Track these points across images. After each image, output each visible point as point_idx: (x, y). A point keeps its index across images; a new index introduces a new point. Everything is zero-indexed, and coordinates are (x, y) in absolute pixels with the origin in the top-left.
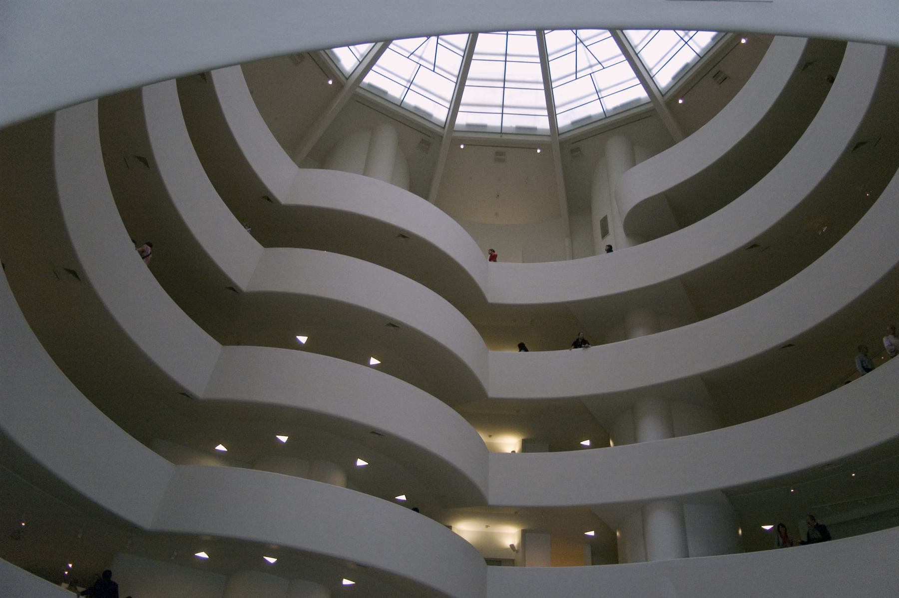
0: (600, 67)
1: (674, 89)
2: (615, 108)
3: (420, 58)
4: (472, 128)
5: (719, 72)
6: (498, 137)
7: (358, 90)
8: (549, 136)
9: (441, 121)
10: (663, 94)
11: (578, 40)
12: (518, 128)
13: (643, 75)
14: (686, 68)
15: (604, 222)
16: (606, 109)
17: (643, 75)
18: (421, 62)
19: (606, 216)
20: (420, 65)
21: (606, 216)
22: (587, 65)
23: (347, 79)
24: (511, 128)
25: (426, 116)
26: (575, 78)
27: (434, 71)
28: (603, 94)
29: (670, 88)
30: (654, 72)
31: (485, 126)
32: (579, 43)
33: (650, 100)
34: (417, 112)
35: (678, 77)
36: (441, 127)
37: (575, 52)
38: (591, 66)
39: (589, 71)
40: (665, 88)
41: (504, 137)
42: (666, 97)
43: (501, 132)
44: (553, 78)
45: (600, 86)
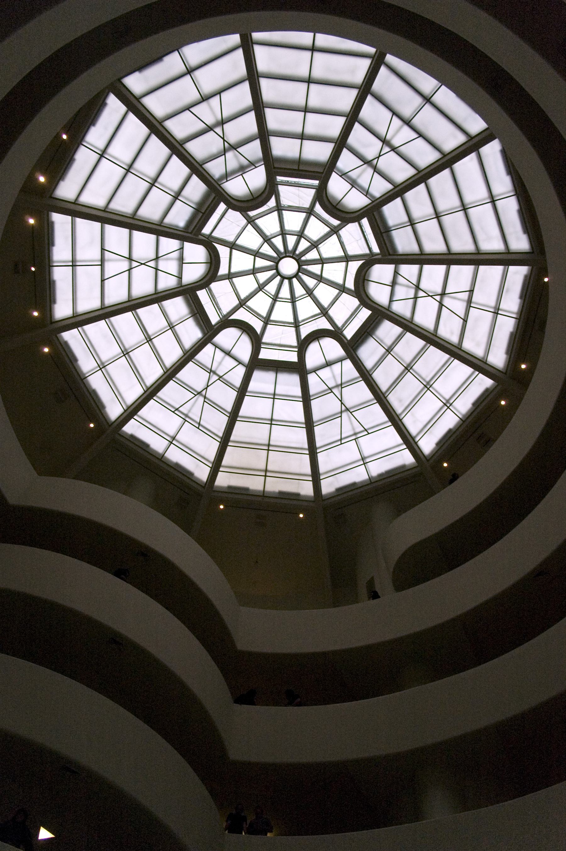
2: (380, 475)
3: (187, 416)
4: (233, 491)
6: (260, 499)
7: (117, 437)
8: (314, 501)
9: (202, 481)
10: (428, 459)
11: (343, 408)
12: (281, 493)
14: (450, 433)
15: (371, 583)
16: (372, 477)
18: (187, 419)
19: (372, 578)
20: (186, 421)
21: (372, 578)
22: (351, 433)
23: (110, 426)
24: (274, 493)
25: (188, 474)
29: (434, 453)
31: (247, 489)
32: (345, 411)
33: (417, 465)
34: (178, 468)
35: (441, 444)
36: (201, 486)
38: (355, 434)
39: (354, 437)
40: (429, 455)
41: (267, 500)
42: (431, 461)
43: (263, 495)
44: (318, 445)
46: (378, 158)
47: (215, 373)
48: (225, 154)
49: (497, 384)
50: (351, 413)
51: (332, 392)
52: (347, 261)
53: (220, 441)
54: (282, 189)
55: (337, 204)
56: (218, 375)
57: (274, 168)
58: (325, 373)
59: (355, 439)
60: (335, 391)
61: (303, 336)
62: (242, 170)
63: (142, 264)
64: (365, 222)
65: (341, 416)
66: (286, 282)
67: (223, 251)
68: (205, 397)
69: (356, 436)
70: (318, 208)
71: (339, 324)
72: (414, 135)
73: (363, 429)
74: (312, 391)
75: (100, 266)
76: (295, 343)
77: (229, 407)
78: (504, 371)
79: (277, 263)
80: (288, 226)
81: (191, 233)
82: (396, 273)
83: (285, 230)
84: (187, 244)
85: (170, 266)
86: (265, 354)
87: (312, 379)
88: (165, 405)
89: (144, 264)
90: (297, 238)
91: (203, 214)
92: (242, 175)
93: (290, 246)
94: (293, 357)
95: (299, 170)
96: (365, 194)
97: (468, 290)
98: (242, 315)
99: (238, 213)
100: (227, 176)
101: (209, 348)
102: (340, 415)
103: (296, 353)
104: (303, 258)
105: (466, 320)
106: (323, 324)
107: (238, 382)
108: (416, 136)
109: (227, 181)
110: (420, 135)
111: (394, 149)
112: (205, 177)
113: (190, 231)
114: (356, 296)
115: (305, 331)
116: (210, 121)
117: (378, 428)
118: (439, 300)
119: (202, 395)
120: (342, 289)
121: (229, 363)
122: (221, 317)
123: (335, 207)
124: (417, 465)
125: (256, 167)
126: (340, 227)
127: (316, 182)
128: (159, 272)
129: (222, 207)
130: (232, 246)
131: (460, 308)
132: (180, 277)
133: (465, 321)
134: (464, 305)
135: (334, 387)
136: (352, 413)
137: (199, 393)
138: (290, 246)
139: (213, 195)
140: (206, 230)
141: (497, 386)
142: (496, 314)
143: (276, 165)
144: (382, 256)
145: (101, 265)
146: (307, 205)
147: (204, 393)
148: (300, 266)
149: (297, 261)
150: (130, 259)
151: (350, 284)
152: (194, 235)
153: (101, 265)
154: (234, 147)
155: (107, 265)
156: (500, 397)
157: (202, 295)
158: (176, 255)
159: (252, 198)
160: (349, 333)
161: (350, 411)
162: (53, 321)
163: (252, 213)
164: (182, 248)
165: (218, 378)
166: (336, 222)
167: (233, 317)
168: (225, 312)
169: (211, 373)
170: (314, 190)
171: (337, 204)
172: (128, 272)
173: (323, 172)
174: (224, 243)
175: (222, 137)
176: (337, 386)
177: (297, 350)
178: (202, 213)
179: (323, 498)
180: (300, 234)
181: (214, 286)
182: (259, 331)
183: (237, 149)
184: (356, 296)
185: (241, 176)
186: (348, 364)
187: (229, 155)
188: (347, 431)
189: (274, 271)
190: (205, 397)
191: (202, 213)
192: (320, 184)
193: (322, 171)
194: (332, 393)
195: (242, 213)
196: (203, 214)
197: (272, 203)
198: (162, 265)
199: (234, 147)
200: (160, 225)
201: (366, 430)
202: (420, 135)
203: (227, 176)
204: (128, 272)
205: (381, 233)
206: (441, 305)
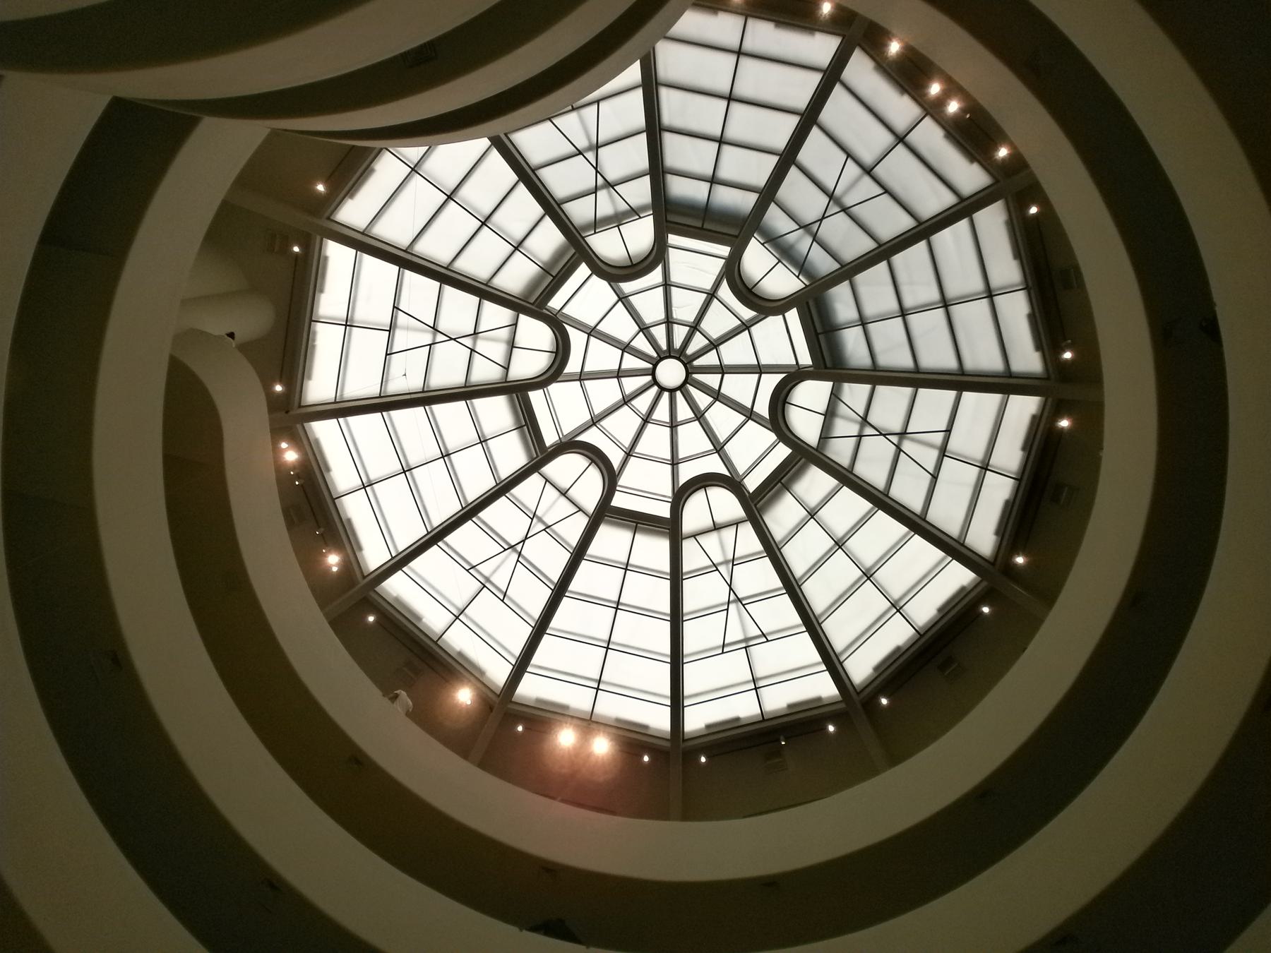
0: (765, 640)
1: (877, 682)
3: (488, 580)
11: (732, 597)
13: (832, 662)
17: (832, 662)
18: (487, 585)
20: (485, 586)
26: (721, 652)
27: (502, 601)
28: (760, 684)
29: (869, 683)
30: (842, 659)
32: (734, 601)
37: (726, 611)
38: (746, 640)
39: (744, 645)
45: (758, 674)
46: (821, 220)
47: (540, 520)
48: (595, 192)
49: (980, 579)
50: (743, 605)
51: (717, 570)
52: (761, 373)
53: (533, 625)
54: (673, 255)
56: (543, 523)
57: (667, 221)
58: (710, 541)
59: (745, 648)
60: (722, 569)
61: (683, 480)
62: (617, 220)
63: (451, 339)
64: (793, 315)
65: (727, 610)
67: (577, 338)
68: (520, 554)
69: (746, 644)
70: (725, 291)
71: (741, 469)
72: (878, 190)
73: (761, 633)
74: (687, 566)
75: (388, 332)
76: (668, 491)
77: (555, 575)
78: (992, 560)
79: (655, 366)
80: (677, 314)
81: (532, 304)
82: (835, 396)
83: (672, 318)
84: (522, 317)
85: (493, 349)
86: (619, 501)
87: (688, 547)
88: (456, 556)
89: (455, 339)
90: (689, 330)
91: (554, 277)
92: (618, 226)
93: (678, 343)
94: (664, 511)
96: (797, 275)
97: (944, 429)
98: (592, 437)
99: (604, 284)
100: (597, 224)
101: (534, 480)
102: (726, 607)
103: (670, 504)
104: (696, 363)
105: (936, 475)
106: (714, 465)
107: (574, 539)
108: (881, 191)
109: (595, 233)
110: (886, 191)
111: (845, 210)
112: (563, 223)
113: (532, 301)
114: (764, 316)
115: (687, 472)
116: (582, 143)
117: (784, 634)
118: (896, 442)
119: (516, 551)
120: (750, 414)
121: (565, 507)
122: (561, 436)
123: (750, 290)
124: (840, 699)
125: (640, 218)
126: (754, 321)
127: (725, 250)
128: (476, 357)
129: (583, 270)
131: (930, 457)
133: (935, 477)
134: (935, 454)
135: (721, 564)
136: (746, 606)
137: (512, 547)
138: (678, 343)
139: (573, 251)
140: (555, 303)
141: (981, 581)
142: (984, 471)
144: (815, 368)
146: (708, 285)
147: (519, 548)
148: (688, 374)
149: (685, 365)
151: (763, 408)
152: (537, 307)
153: (389, 331)
154: (610, 185)
155: (399, 334)
156: (983, 598)
157: (536, 397)
158: (505, 333)
159: (630, 264)
160: (752, 483)
161: (741, 603)
162: (303, 404)
163: (627, 287)
164: (515, 325)
165: (544, 527)
166: (747, 314)
167: (581, 438)
168: (567, 429)
169: (535, 520)
170: (724, 261)
172: (429, 347)
173: (739, 234)
175: (595, 166)
176: (726, 562)
177: (671, 500)
178: (552, 276)
179: (686, 737)
180: (694, 325)
181: (554, 388)
182: (616, 464)
183: (615, 187)
184: (764, 316)
185: (617, 228)
186: (747, 530)
187: (602, 194)
188: (735, 634)
189: (649, 378)
190: (520, 554)
191: (552, 276)
192: (731, 254)
193: (737, 234)
194: (717, 572)
195: (612, 283)
196: (554, 277)
197: (656, 276)
198: (481, 346)
199: (610, 185)
200: (486, 285)
201: (764, 635)
202: (886, 191)
203: (597, 224)
204: (429, 347)
206: (899, 450)
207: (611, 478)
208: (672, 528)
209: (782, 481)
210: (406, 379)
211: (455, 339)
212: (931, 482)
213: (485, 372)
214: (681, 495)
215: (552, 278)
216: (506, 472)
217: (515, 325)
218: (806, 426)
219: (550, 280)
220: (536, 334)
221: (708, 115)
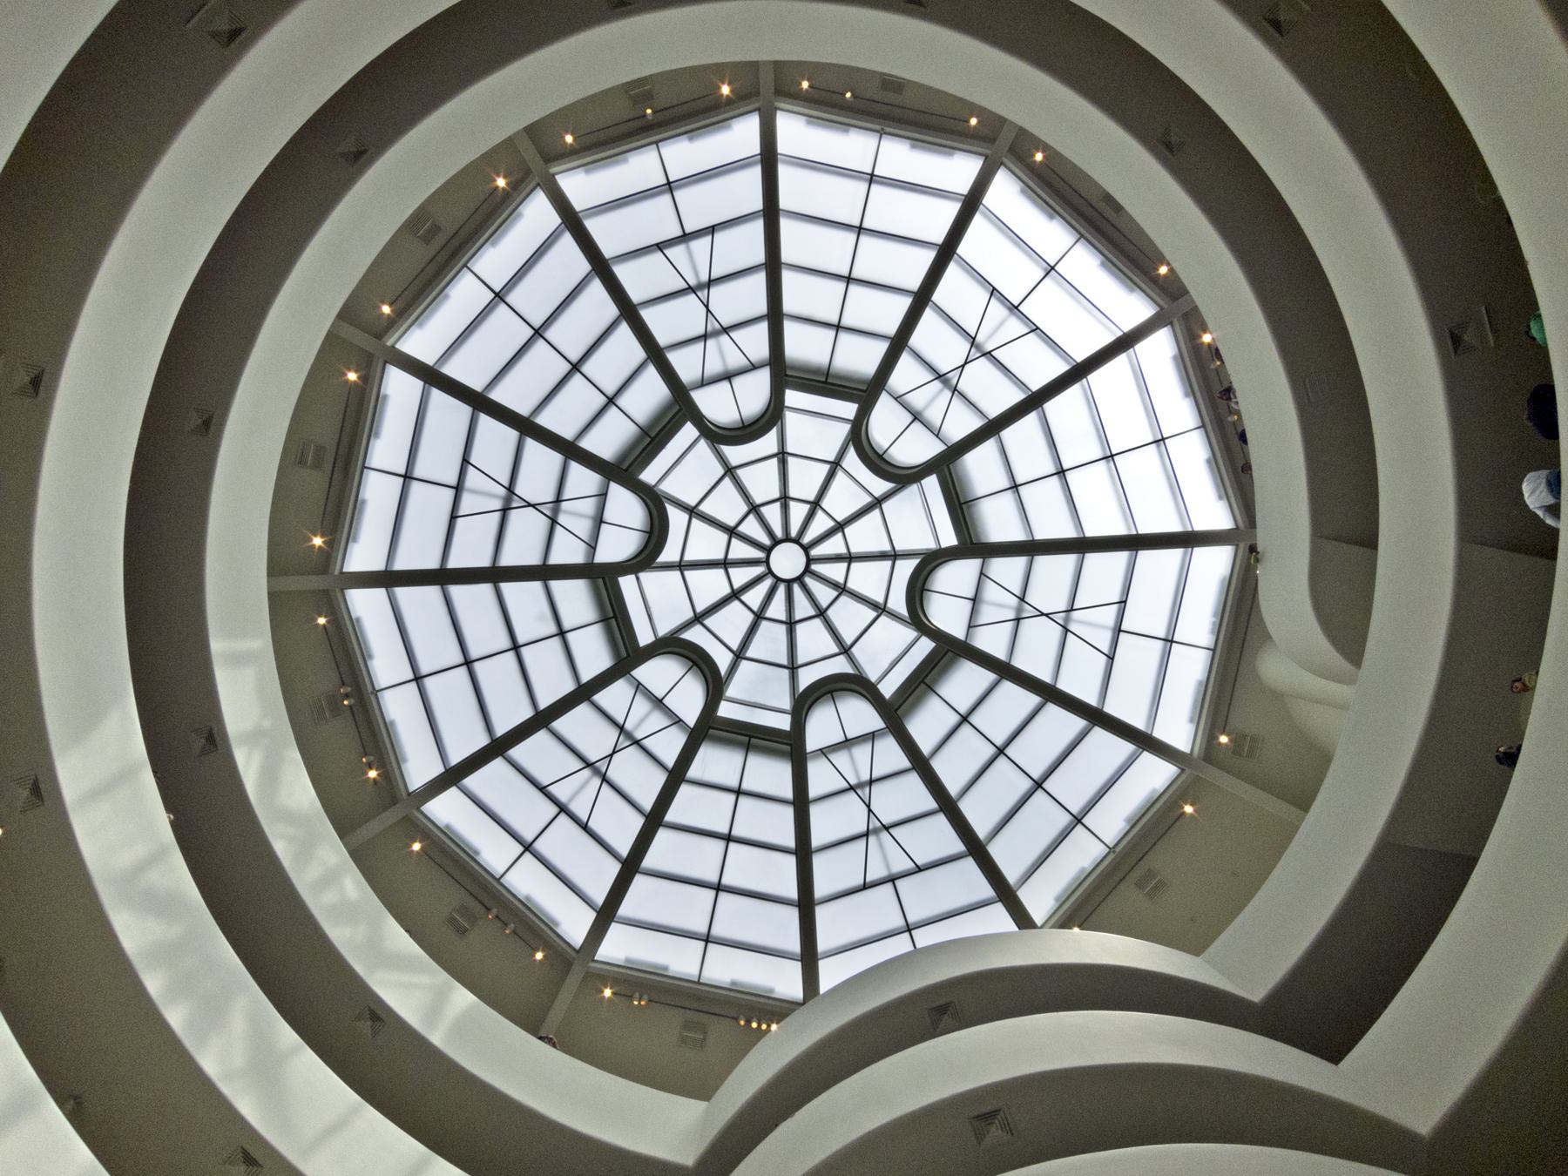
5: (427, 239)
55: (692, 667)
66: (794, 533)
72: (553, 789)
94: (793, 397)
95: (750, 737)
107: (905, 361)
108: (552, 789)
112: (908, 744)
115: (767, 443)
130: (881, 609)
132: (982, 576)
143: (788, 748)
145: (1120, 631)
150: (1066, 630)
153: (1120, 631)
171: (692, 667)
172: (1075, 607)
174: (895, 616)
182: (852, 453)
204: (1075, 607)
205: (615, 617)
207: (858, 437)
208: (783, 373)
209: (649, 439)
210: (1105, 569)
211: (1042, 614)
212: (469, 455)
213: (1008, 570)
214: (773, 415)
215: (926, 681)
216: (988, 448)
217: (970, 627)
218: (625, 507)
219: (928, 678)
220: (947, 615)
221: (744, 867)
